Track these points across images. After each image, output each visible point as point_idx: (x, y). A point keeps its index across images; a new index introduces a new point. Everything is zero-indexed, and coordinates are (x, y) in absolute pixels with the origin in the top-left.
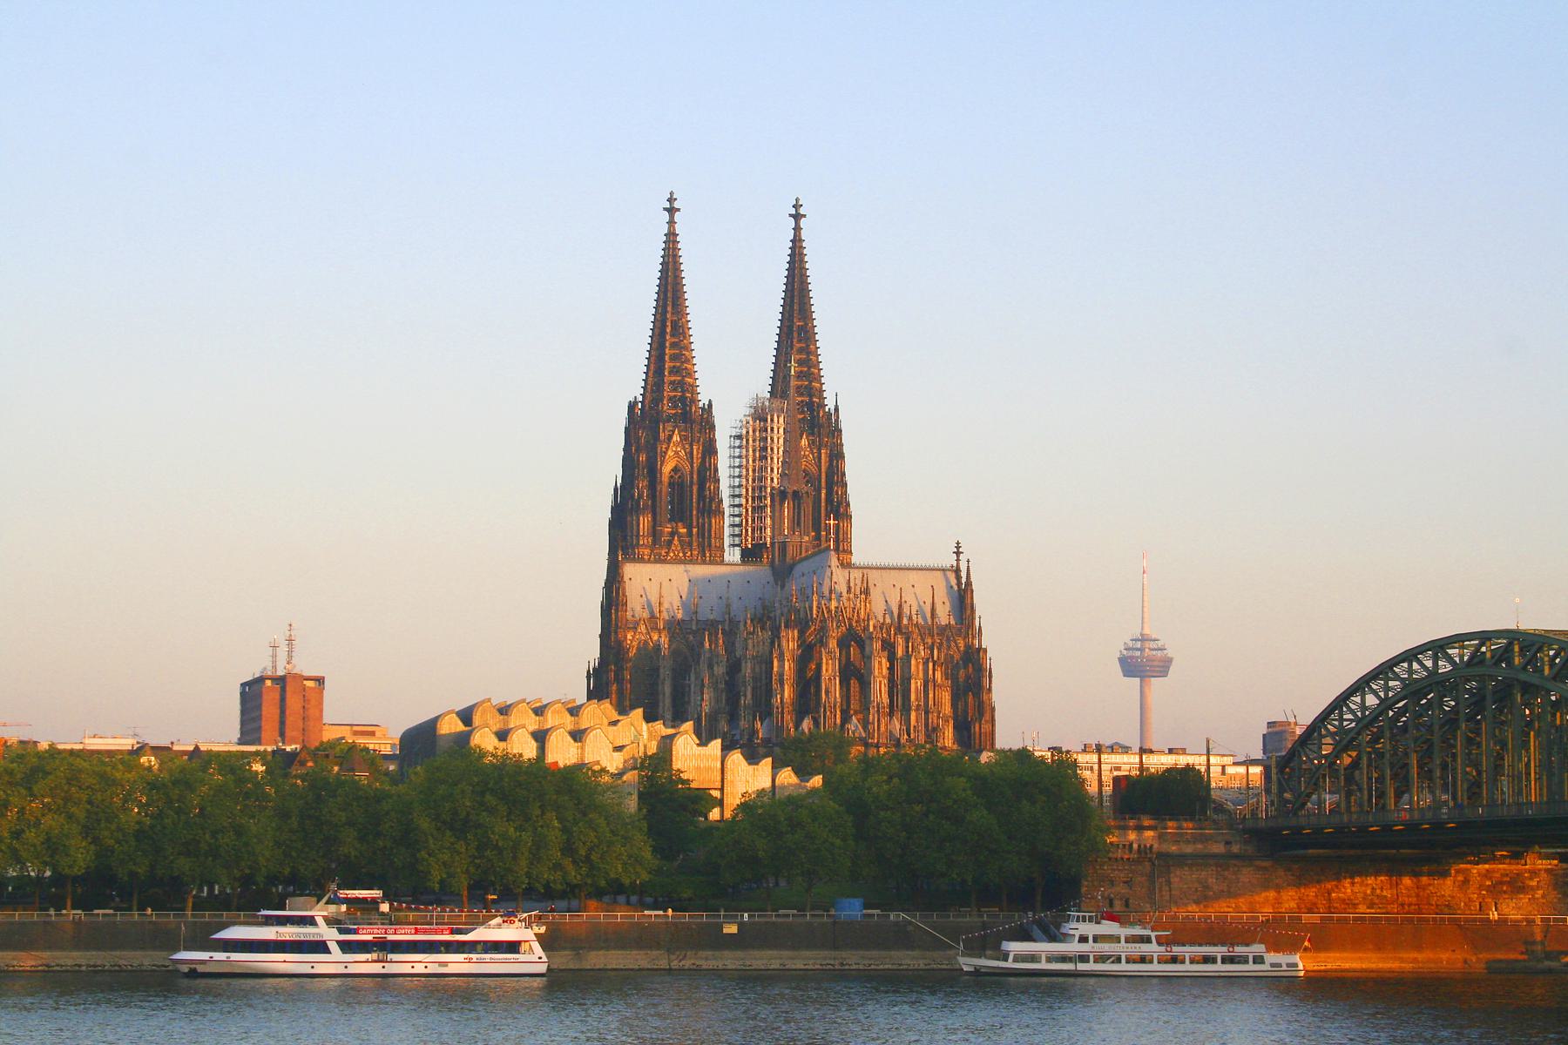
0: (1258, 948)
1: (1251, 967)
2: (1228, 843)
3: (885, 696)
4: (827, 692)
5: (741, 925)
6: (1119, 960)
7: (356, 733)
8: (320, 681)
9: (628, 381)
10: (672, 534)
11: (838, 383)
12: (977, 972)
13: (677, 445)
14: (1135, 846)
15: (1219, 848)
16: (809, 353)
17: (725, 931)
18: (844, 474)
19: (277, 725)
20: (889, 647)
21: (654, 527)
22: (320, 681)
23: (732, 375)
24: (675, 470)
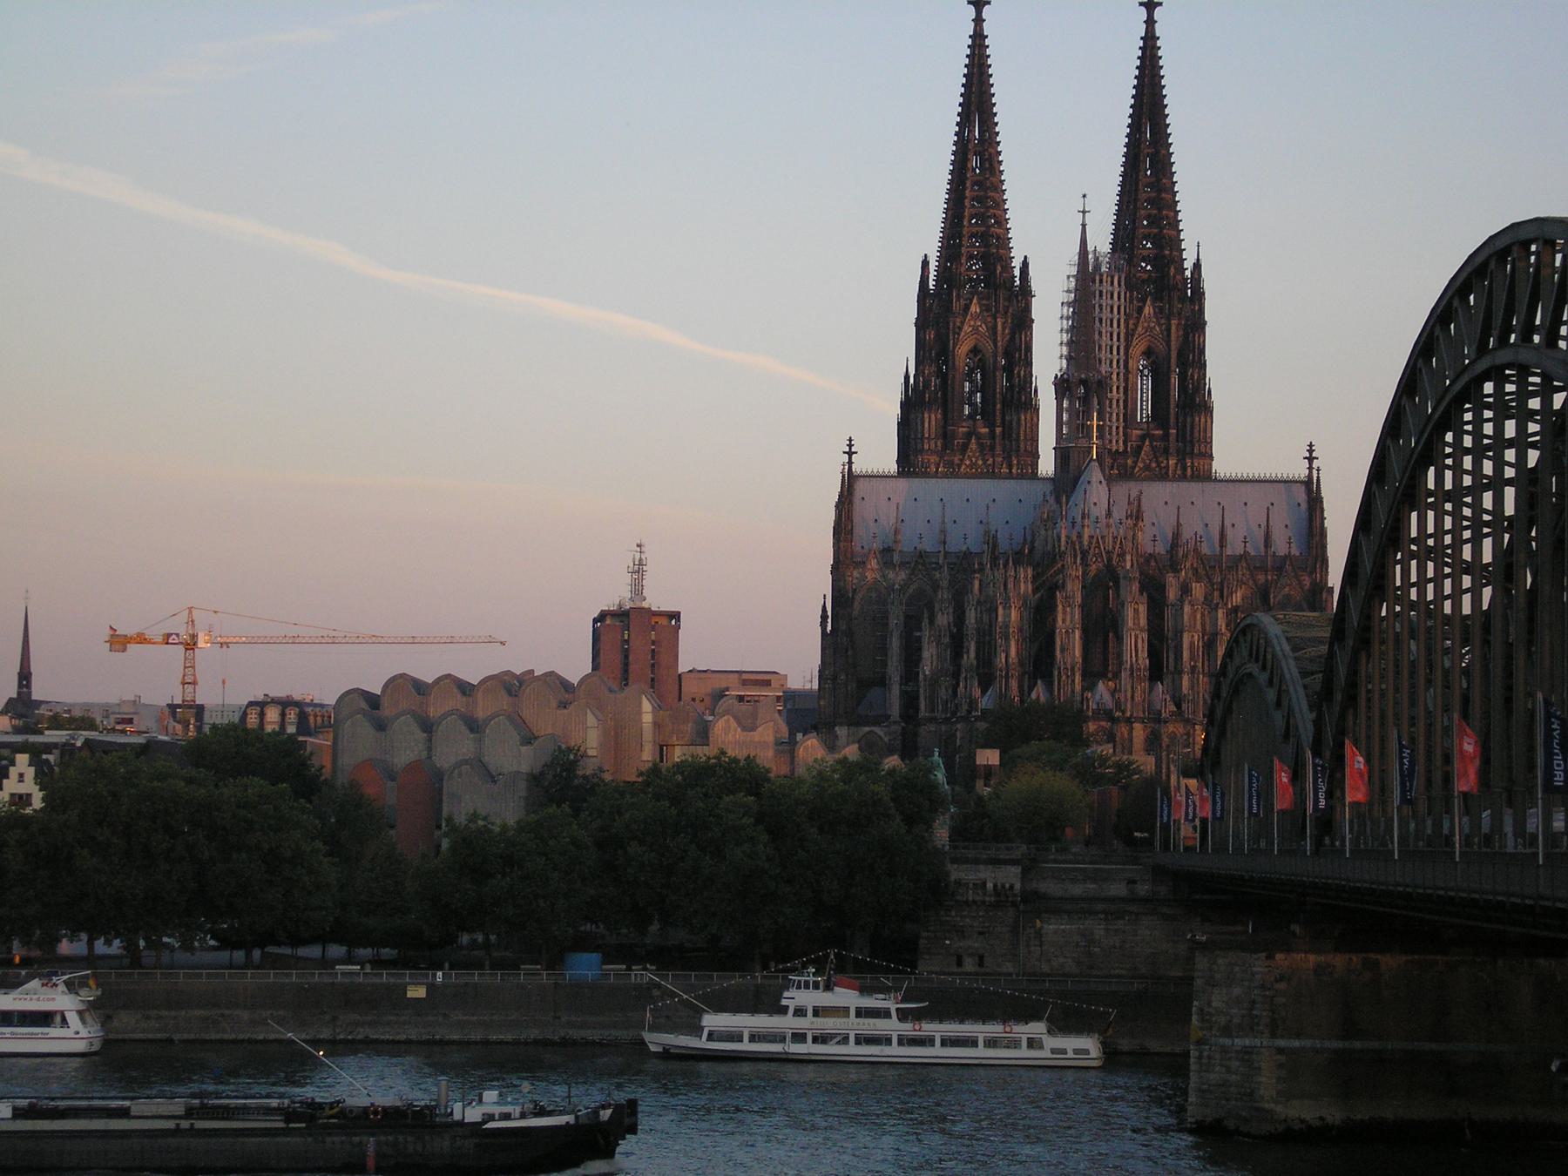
0: (1037, 1028)
1: (1024, 1052)
2: (1132, 882)
3: (1143, 654)
4: (1063, 650)
5: (431, 988)
6: (845, 1040)
7: (745, 683)
8: (676, 616)
9: (921, 232)
10: (969, 435)
11: (1202, 228)
12: (667, 1054)
13: (976, 317)
14: (990, 885)
15: (1117, 889)
16: (1160, 191)
17: (410, 994)
18: (1202, 352)
19: (631, 668)
20: (1154, 591)
21: (944, 427)
22: (676, 616)
23: (1057, 220)
24: (975, 351)
